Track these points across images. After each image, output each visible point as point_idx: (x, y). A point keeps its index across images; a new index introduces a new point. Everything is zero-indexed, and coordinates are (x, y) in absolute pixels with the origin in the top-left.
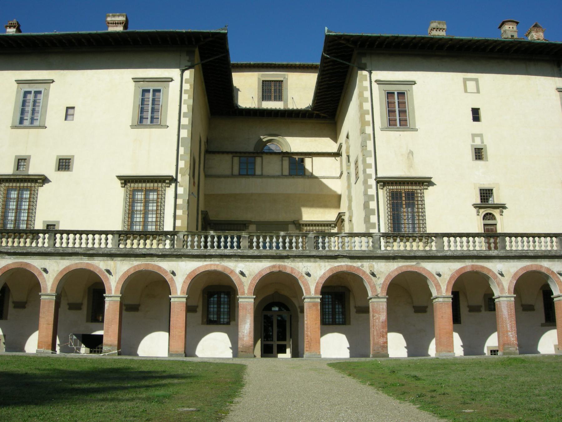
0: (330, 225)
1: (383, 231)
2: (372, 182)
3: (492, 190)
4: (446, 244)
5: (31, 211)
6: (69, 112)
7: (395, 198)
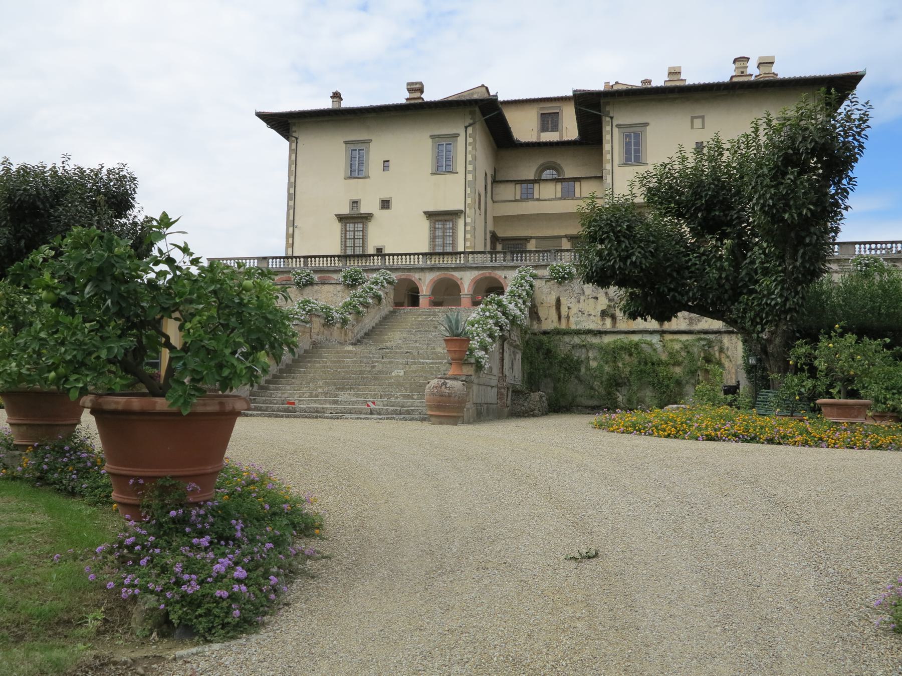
5: (364, 239)
6: (386, 165)
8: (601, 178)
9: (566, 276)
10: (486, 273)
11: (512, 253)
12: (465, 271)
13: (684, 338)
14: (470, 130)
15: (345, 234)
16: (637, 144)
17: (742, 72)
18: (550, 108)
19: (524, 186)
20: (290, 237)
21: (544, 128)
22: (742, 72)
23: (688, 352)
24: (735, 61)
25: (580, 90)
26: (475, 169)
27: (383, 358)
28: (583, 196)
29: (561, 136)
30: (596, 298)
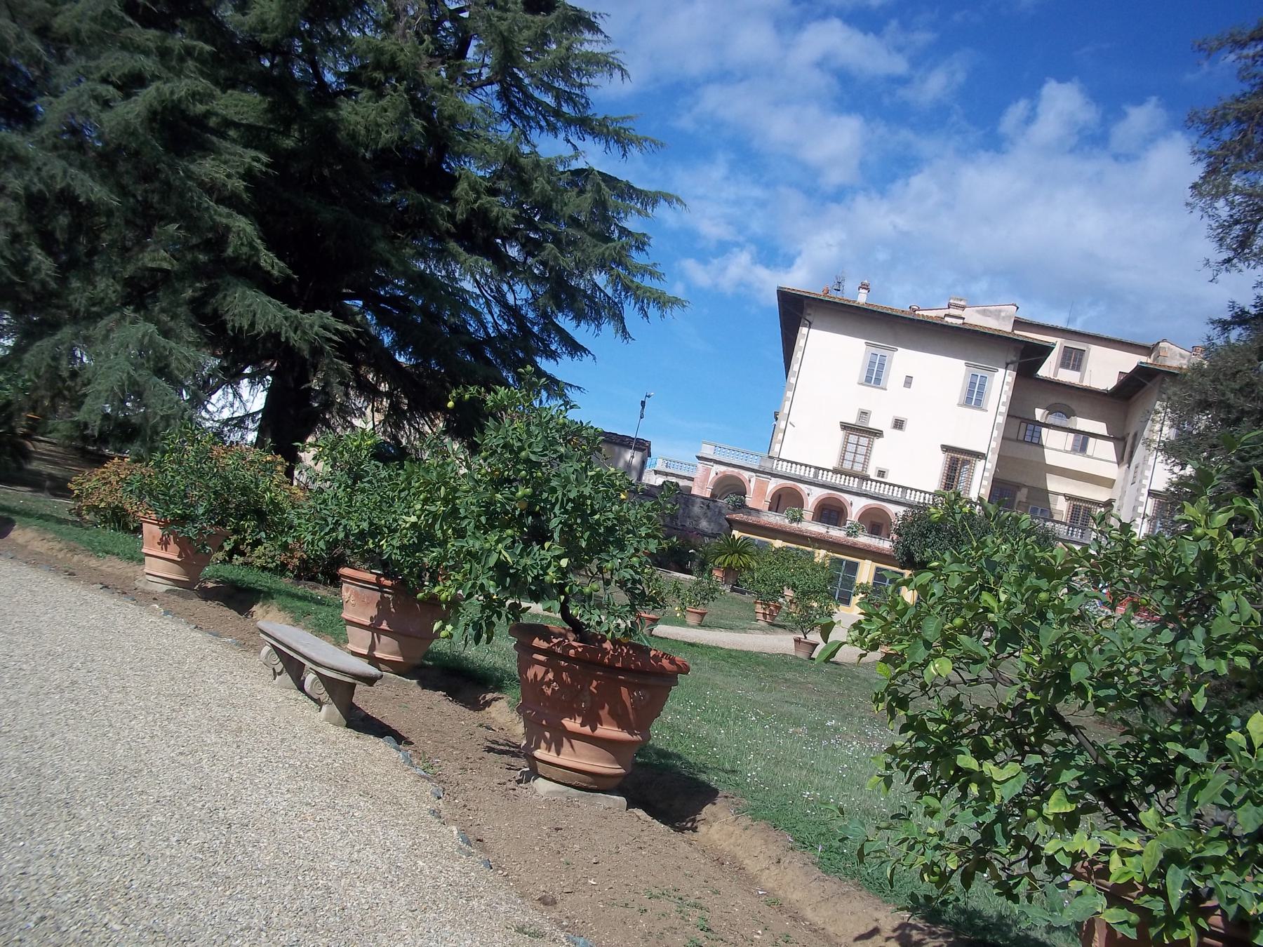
2: (1145, 492)
5: (867, 456)
6: (908, 381)
29: (1082, 379)
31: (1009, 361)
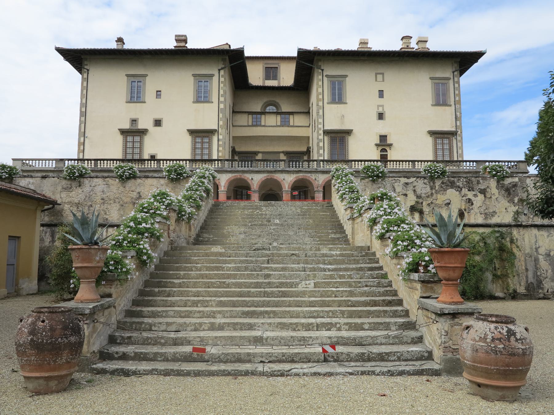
0: (303, 153)
1: (326, 158)
2: (321, 132)
3: (386, 136)
4: (353, 165)
5: (141, 148)
6: (158, 94)
7: (333, 141)
8: (308, 113)
9: (380, 175)
10: (238, 175)
11: (242, 161)
12: (222, 173)
13: (481, 230)
14: (222, 72)
15: (126, 144)
16: (340, 89)
17: (408, 46)
18: (271, 64)
19: (255, 116)
20: (82, 145)
21: (267, 77)
22: (408, 46)
23: (485, 243)
24: (402, 39)
25: (303, 49)
26: (225, 100)
27: (268, 263)
28: (295, 125)
30: (406, 195)
31: (220, 68)
